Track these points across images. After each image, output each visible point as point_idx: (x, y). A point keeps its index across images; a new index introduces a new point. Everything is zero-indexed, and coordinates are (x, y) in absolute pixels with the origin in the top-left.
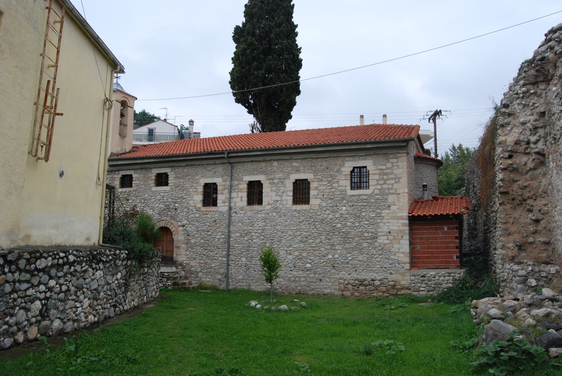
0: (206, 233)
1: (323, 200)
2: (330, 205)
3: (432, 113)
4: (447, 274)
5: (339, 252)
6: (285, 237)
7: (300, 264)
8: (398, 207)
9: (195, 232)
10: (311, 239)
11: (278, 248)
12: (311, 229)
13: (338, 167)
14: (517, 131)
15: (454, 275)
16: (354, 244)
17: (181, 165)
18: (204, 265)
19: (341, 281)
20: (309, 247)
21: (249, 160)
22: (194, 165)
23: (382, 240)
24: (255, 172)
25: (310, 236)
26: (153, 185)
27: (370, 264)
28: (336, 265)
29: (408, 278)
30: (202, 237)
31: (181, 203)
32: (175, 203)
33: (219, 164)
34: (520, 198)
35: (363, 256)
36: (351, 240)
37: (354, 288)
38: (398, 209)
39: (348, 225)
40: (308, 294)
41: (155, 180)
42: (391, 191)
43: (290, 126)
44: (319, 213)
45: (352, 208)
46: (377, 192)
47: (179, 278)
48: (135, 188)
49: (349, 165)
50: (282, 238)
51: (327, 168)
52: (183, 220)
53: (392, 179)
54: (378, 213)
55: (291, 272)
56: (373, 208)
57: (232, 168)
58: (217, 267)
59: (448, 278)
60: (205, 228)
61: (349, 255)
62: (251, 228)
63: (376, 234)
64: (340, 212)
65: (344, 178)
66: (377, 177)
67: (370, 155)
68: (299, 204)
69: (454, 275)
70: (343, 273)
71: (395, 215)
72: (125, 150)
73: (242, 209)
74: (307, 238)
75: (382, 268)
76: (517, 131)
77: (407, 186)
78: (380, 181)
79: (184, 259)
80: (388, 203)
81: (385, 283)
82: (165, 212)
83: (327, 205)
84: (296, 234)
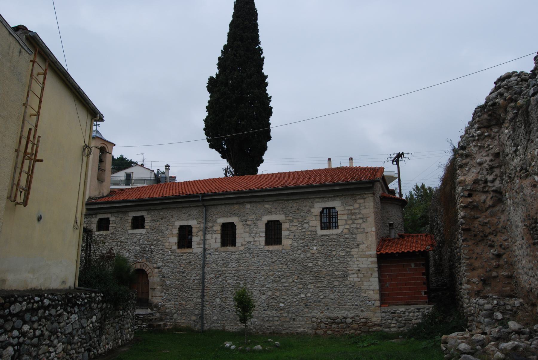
0: (181, 274)
1: (295, 240)
2: (302, 245)
3: (395, 156)
4: (416, 310)
5: (311, 290)
6: (258, 277)
7: (273, 303)
8: (366, 245)
10: (284, 278)
11: (251, 289)
12: (283, 269)
13: (308, 208)
14: (475, 171)
15: (423, 310)
16: (326, 283)
18: (178, 306)
19: (314, 319)
20: (281, 286)
22: (170, 208)
23: (353, 278)
25: (282, 275)
26: (130, 228)
27: (342, 302)
28: (308, 304)
29: (379, 314)
30: (177, 278)
31: (157, 245)
32: (151, 245)
33: (194, 207)
34: (481, 234)
35: (334, 294)
36: (322, 279)
37: (326, 327)
38: (367, 247)
39: (319, 264)
40: (282, 334)
41: (132, 223)
42: (359, 230)
43: (262, 169)
44: (291, 253)
45: (323, 247)
46: (346, 231)
47: (154, 320)
48: (112, 231)
49: (318, 207)
50: (255, 279)
51: (298, 210)
52: (159, 261)
53: (360, 218)
54: (347, 252)
55: (264, 312)
56: (342, 247)
57: (207, 210)
58: (192, 308)
59: (417, 313)
60: (180, 270)
61: (321, 294)
62: (225, 269)
63: (346, 272)
64: (311, 251)
65: (314, 219)
66: (345, 217)
67: (338, 196)
68: (272, 245)
69: (423, 310)
70: (315, 311)
71: (364, 253)
72: (103, 194)
73: (216, 250)
74: (279, 278)
75: (353, 305)
76: (475, 171)
77: (374, 225)
78: (348, 221)
80: (356, 242)
81: (357, 321)
82: (141, 254)
83: (298, 245)
84: (269, 274)
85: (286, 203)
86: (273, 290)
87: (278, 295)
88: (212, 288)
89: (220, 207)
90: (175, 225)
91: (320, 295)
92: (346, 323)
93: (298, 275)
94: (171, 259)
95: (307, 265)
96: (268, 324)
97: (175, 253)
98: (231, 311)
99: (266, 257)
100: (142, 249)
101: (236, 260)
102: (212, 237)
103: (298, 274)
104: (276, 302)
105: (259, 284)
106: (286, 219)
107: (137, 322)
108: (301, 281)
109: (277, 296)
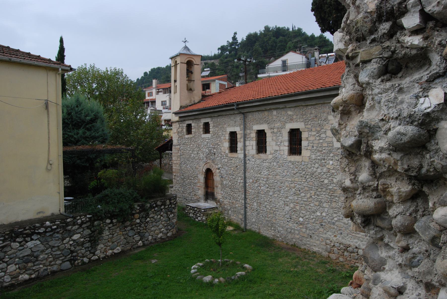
0: (232, 176)
1: (313, 152)
2: (319, 158)
6: (283, 188)
7: (294, 216)
9: (225, 175)
11: (278, 198)
12: (303, 183)
17: (215, 116)
19: (328, 241)
20: (301, 200)
21: (255, 110)
24: (261, 121)
25: (302, 189)
26: (202, 133)
28: (324, 224)
31: (217, 149)
32: (214, 148)
36: (337, 199)
39: (335, 182)
40: (300, 248)
41: (203, 128)
50: (281, 188)
51: (316, 117)
55: (288, 223)
58: (239, 208)
61: (335, 215)
62: (260, 175)
64: (327, 166)
70: (329, 233)
72: (194, 101)
73: (253, 156)
74: (300, 191)
79: (221, 197)
82: (209, 155)
84: (291, 185)
85: (305, 109)
89: (255, 114)
90: (227, 131)
91: (334, 216)
92: (358, 255)
93: (315, 191)
94: (226, 162)
95: (323, 181)
96: (290, 236)
103: (315, 190)
104: (296, 215)
106: (305, 128)
108: (318, 197)
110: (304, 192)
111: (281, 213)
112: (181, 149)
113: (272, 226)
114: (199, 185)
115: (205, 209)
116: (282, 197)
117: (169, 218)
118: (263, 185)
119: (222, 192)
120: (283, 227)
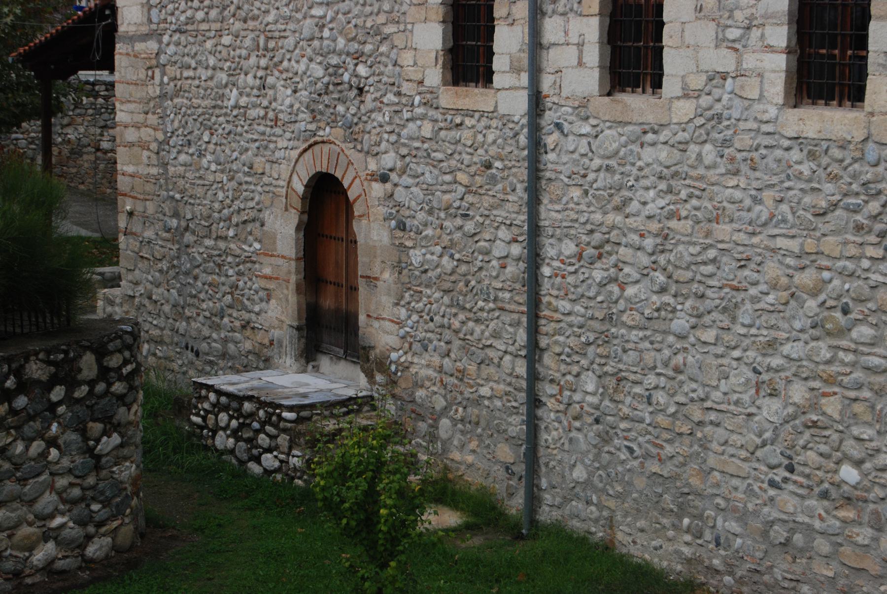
0: (459, 221)
6: (753, 291)
9: (421, 216)
11: (720, 350)
12: (866, 264)
18: (453, 380)
20: (854, 364)
31: (374, 61)
32: (358, 57)
50: (740, 296)
52: (384, 145)
55: (772, 492)
58: (498, 403)
62: (619, 219)
73: (582, 108)
74: (846, 311)
82: (326, 98)
86: (814, 379)
87: (836, 416)
88: (569, 314)
94: (424, 140)
96: (785, 566)
97: (437, 108)
98: (638, 452)
99: (788, 178)
100: (330, 75)
101: (660, 178)
102: (566, 33)
104: (823, 448)
105: (753, 331)
107: (276, 437)
109: (830, 417)
110: (873, 320)
111: (734, 437)
112: (163, 59)
113: (682, 510)
114: (267, 271)
115: (303, 407)
116: (747, 342)
117: (98, 458)
118: (636, 276)
119: (403, 312)
120: (743, 517)
